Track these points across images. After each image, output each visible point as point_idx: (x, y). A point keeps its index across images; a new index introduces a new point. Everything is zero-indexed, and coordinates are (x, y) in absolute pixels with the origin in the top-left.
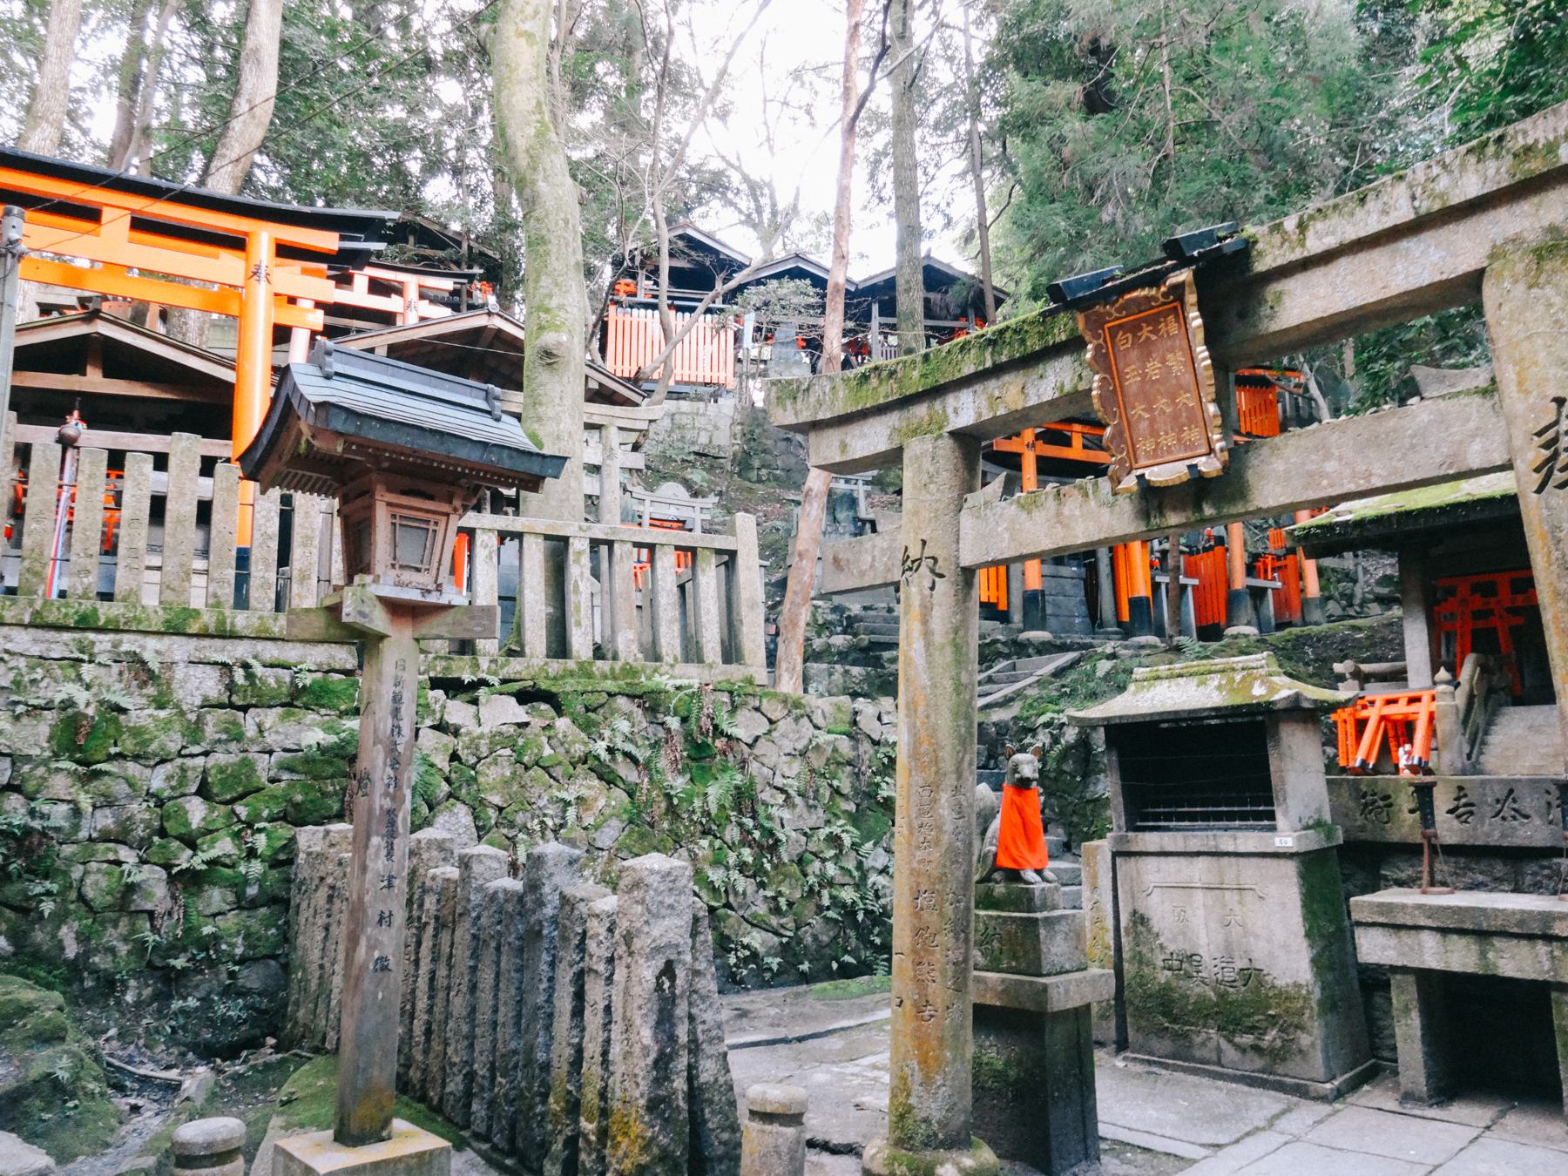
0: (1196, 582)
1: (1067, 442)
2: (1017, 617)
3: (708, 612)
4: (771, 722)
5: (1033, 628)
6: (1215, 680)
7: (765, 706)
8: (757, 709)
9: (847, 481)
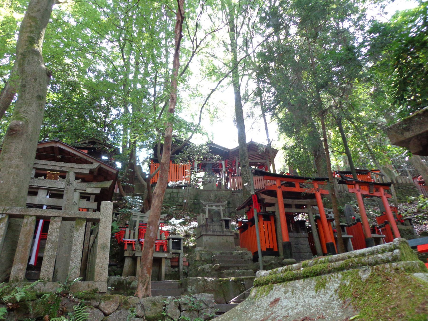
0: (352, 236)
1: (294, 186)
2: (281, 253)
3: (76, 252)
4: (105, 315)
5: (287, 258)
6: (334, 282)
7: (103, 304)
8: (97, 307)
9: (217, 206)
